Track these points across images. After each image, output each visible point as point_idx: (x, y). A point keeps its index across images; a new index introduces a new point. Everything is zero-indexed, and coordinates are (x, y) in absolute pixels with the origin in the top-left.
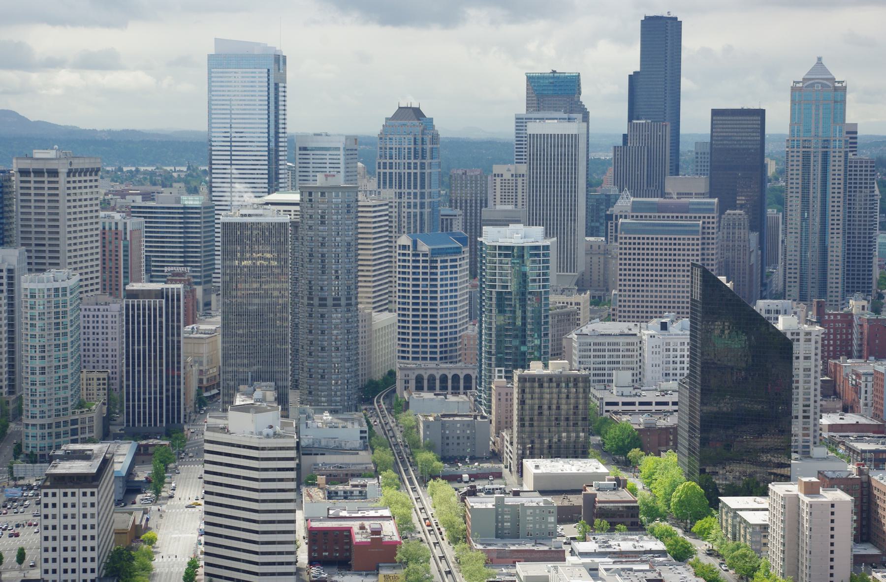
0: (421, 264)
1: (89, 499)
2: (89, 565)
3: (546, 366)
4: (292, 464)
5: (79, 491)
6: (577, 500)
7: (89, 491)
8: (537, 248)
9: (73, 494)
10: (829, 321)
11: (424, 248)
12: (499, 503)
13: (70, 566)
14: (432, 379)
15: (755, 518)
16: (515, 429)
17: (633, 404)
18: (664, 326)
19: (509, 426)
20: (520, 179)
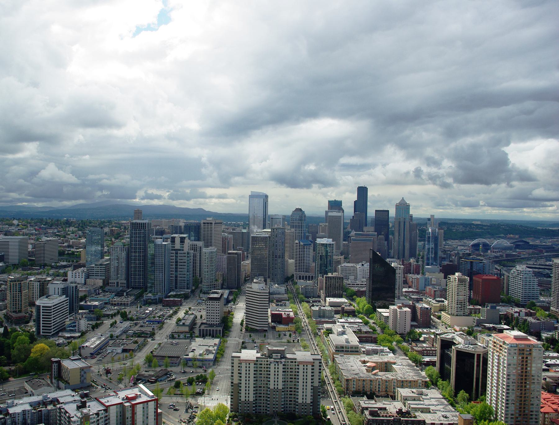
0: (301, 248)
1: (218, 304)
2: (217, 320)
3: (332, 274)
4: (268, 297)
5: (215, 302)
6: (340, 309)
7: (218, 302)
8: (330, 244)
9: (214, 302)
10: (405, 264)
11: (302, 243)
12: (320, 308)
13: (213, 320)
14: (303, 277)
16: (324, 290)
17: (354, 284)
18: (363, 265)
19: (322, 289)
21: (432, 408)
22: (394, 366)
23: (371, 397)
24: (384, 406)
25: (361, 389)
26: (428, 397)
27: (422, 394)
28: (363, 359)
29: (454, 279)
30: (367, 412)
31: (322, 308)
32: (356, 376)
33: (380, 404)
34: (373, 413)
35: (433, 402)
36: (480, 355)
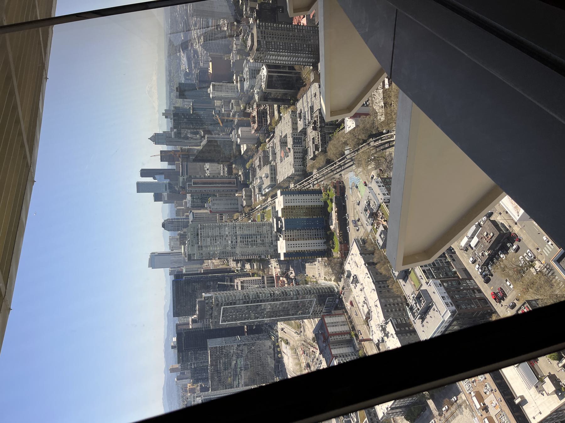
7: (244, 282)
12: (244, 200)
15: (245, 148)
18: (208, 169)
20: (178, 202)
21: (310, 105)
22: (282, 137)
23: (305, 152)
24: (311, 140)
25: (301, 160)
26: (303, 109)
27: (300, 114)
28: (279, 161)
29: (213, 94)
30: (317, 152)
31: (244, 197)
32: (292, 164)
33: (310, 144)
34: (317, 148)
35: (305, 104)
36: (269, 71)
